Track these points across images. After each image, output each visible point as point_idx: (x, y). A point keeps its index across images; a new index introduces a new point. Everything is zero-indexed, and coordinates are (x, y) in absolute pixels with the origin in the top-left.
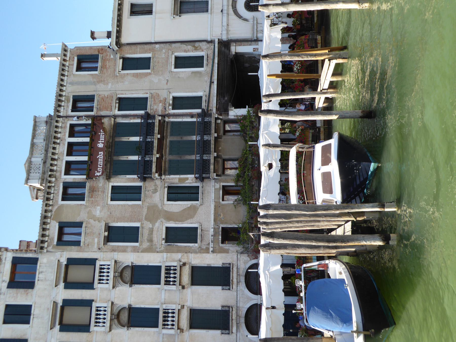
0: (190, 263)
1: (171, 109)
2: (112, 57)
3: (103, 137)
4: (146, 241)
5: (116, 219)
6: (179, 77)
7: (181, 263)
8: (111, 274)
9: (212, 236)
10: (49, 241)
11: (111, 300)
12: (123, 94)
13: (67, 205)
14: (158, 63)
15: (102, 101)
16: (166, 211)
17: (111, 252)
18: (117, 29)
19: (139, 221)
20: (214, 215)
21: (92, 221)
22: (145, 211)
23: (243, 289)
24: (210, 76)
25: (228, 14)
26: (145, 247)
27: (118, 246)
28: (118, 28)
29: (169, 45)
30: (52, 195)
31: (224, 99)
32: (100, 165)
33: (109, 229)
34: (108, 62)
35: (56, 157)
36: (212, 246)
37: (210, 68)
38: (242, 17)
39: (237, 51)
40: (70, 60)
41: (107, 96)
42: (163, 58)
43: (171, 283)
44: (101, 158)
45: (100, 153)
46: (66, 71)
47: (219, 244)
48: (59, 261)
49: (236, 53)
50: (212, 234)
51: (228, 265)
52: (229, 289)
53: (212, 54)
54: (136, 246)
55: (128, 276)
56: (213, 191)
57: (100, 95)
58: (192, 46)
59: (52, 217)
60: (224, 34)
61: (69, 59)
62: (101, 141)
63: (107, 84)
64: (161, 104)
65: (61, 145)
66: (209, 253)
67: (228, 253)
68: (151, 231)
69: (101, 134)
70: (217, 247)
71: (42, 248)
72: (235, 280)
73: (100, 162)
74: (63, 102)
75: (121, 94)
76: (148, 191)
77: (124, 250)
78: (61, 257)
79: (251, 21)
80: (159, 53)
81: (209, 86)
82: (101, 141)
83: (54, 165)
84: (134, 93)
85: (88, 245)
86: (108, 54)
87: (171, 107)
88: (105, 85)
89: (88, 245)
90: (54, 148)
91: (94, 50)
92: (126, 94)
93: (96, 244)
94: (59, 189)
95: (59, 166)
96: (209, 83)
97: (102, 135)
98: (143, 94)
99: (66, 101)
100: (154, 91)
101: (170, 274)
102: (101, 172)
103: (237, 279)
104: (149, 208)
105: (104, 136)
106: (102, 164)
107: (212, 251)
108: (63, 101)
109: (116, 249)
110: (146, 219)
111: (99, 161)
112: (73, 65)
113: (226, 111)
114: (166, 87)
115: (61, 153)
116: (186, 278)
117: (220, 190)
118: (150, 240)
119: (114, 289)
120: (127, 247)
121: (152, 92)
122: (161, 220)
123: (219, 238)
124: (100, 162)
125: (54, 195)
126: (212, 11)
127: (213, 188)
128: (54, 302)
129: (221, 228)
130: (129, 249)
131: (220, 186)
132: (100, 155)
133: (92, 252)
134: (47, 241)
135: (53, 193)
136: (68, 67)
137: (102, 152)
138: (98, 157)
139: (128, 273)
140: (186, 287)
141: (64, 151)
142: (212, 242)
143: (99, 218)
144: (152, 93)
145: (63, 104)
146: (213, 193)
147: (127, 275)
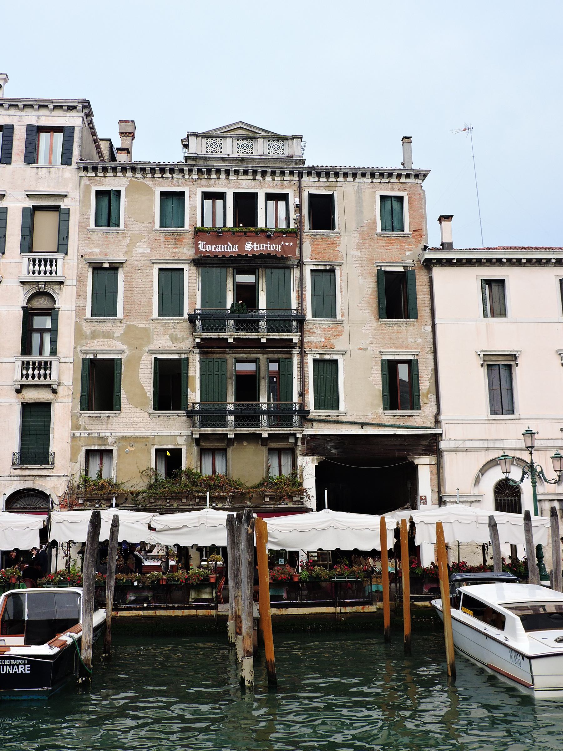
0: (56, 400)
1: (314, 358)
2: (408, 253)
3: (263, 247)
4: (94, 328)
5: (129, 278)
6: (372, 368)
7: (55, 387)
8: (42, 278)
9: (99, 434)
10: (97, 178)
11: (3, 280)
12: (341, 276)
13: (153, 201)
14: (398, 332)
15: (328, 243)
16: (140, 358)
17: (78, 275)
18: (454, 259)
19: (125, 315)
20: (132, 437)
21: (127, 241)
22: (141, 324)
23: (13, 486)
24: (374, 422)
25: (487, 450)
26: (83, 327)
27: (86, 285)
28: (455, 261)
29: (430, 349)
30: (170, 176)
31: (333, 447)
32: (215, 248)
33: (114, 268)
34: (398, 247)
35: (232, 177)
36: (82, 435)
37: (389, 421)
38: (482, 475)
39: (419, 467)
40: (400, 185)
41: (338, 251)
42: (407, 340)
43: (25, 372)
44: (227, 249)
45: (237, 246)
46: (381, 179)
47: (85, 445)
48: (66, 196)
49: (417, 465)
50: (101, 434)
51: (51, 460)
52: (13, 464)
53: (415, 425)
54: (85, 314)
55: (40, 304)
56: (172, 434)
57: (338, 238)
58: (429, 388)
59: (135, 180)
60: (449, 443)
61: (402, 183)
62: (257, 247)
63: (359, 249)
64: (323, 340)
65: (253, 183)
66: (71, 430)
67: (71, 460)
68: (109, 336)
69: (269, 245)
70: (81, 443)
71: (86, 169)
72: (27, 473)
73: (221, 247)
74: (326, 180)
75: (341, 273)
76: (174, 328)
77: (80, 295)
78: (72, 198)
79: (476, 491)
80: (417, 333)
81: (356, 421)
82: (257, 247)
83: (218, 175)
84: (343, 294)
85: (89, 238)
86: (413, 247)
87: (318, 357)
88: (357, 245)
89: (89, 238)
90: (246, 173)
91: (419, 223)
92: (341, 280)
93: (90, 251)
94: (178, 186)
95: (217, 181)
96: (361, 421)
97: (266, 247)
98: (341, 309)
99: (328, 184)
100: (346, 328)
101: (39, 370)
102: (204, 250)
103: (29, 476)
104: (146, 329)
105: (265, 249)
106: (217, 250)
107: (74, 434)
108: (328, 180)
109: (82, 283)
110: (128, 326)
111: (223, 246)
112: (392, 190)
113: (310, 452)
114: (354, 347)
115: (239, 184)
116: (32, 396)
117: (174, 445)
118: (94, 336)
119: (20, 284)
120: (85, 299)
121: (345, 324)
122: (126, 351)
123: (95, 445)
124: (221, 247)
125: (170, 179)
126: (494, 422)
127: (176, 434)
128: (4, 195)
129: (111, 448)
130: (81, 303)
131: (181, 445)
132: (233, 247)
133: (78, 244)
134: (96, 175)
135: (172, 178)
136: (388, 183)
137: (237, 250)
138: (229, 243)
139: (45, 303)
140: (20, 395)
141: (242, 188)
142: (89, 434)
143: (132, 252)
144: (343, 325)
145: (323, 179)
146: (169, 434)
147: (41, 302)
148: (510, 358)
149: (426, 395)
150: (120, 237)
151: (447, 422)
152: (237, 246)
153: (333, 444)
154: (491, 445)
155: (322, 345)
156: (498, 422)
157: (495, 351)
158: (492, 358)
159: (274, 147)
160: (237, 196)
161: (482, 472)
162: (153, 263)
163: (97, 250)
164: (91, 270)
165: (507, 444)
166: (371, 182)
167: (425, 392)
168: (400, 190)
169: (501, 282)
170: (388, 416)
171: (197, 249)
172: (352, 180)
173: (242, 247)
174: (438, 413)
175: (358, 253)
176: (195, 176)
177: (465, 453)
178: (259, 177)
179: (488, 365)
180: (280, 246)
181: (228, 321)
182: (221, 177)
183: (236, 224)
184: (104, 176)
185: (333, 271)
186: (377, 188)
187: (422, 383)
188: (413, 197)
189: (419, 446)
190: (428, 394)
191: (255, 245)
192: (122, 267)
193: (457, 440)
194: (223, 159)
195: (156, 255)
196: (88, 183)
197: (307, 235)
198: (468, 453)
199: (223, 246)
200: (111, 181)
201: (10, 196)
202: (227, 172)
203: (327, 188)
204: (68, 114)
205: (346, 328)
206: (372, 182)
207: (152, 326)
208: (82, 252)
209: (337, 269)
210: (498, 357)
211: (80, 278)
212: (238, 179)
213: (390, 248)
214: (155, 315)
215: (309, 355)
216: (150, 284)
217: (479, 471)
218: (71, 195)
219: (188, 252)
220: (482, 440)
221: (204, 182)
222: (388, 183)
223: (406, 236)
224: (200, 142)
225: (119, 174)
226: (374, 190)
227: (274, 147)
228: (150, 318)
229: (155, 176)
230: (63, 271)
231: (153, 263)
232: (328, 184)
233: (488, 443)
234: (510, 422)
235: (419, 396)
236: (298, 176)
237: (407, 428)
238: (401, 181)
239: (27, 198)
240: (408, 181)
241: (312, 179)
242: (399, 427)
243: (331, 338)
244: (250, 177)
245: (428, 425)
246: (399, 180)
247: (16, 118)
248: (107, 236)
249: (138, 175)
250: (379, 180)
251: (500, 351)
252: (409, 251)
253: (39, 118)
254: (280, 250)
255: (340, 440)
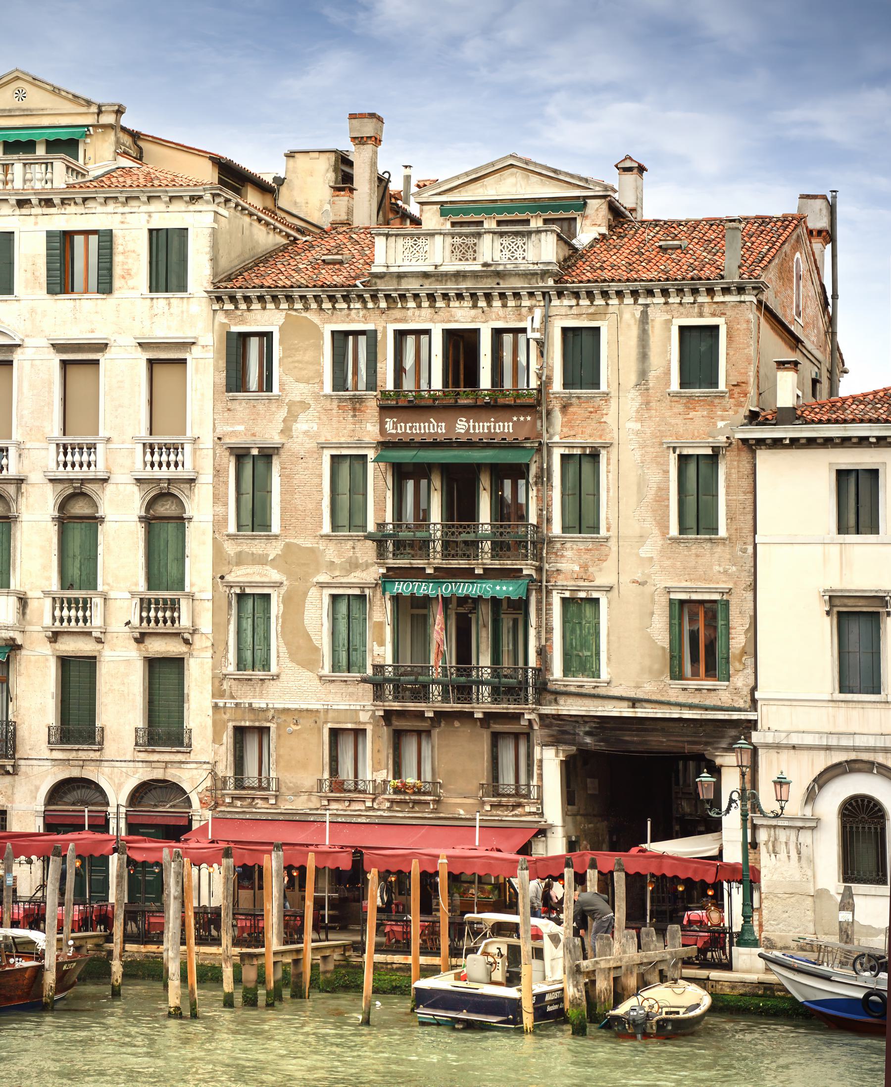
0: (191, 655)
1: (563, 596)
2: (720, 424)
3: (483, 429)
4: (239, 549)
5: (287, 472)
6: (652, 614)
7: (187, 636)
8: (164, 473)
9: (250, 704)
10: (239, 313)
11: (112, 476)
12: (608, 464)
13: (319, 348)
14: (697, 556)
15: (590, 409)
16: (305, 594)
17: (214, 468)
19: (284, 527)
20: (296, 710)
21: (283, 413)
22: (307, 542)
23: (137, 776)
24: (654, 698)
25: (828, 748)
26: (225, 546)
27: (226, 483)
29: (749, 583)
30: (345, 306)
31: (588, 733)
32: (411, 428)
33: (267, 455)
34: (705, 413)
35: (440, 304)
36: (228, 705)
37: (677, 697)
38: (820, 788)
39: (723, 770)
40: (715, 306)
41: (605, 422)
42: (712, 569)
43: (144, 614)
44: (429, 429)
45: (443, 424)
46: (682, 298)
47: (233, 721)
48: (194, 343)
49: (722, 766)
50: (254, 705)
51: (186, 741)
52: (136, 745)
53: (719, 703)
54: (227, 526)
55: (166, 509)
56: (352, 707)
57: (606, 401)
58: (744, 647)
59: (294, 313)
60: (765, 737)
61: (717, 303)
62: (474, 427)
63: (640, 420)
64: (577, 568)
65: (473, 312)
66: (213, 696)
67: (214, 741)
68: (261, 560)
69: (492, 424)
70: (226, 717)
71: (219, 299)
72: (155, 757)
73: (420, 427)
74: (588, 303)
75: (608, 459)
76: (354, 548)
77: (218, 498)
78: (203, 347)
79: (808, 812)
80: (728, 556)
81: (624, 695)
82: (474, 427)
83: (418, 300)
84: (611, 494)
85: (229, 410)
86: (731, 413)
87: (567, 594)
88: (637, 412)
89: (229, 410)
90: (460, 297)
91: (743, 371)
92: (608, 472)
93: (231, 429)
94: (359, 322)
95: (417, 312)
96: (632, 694)
97: (489, 428)
98: (607, 518)
99: (592, 310)
100: (614, 549)
101: (165, 611)
102: (394, 431)
103: (158, 762)
104: (312, 550)
105: (486, 431)
106: (414, 432)
107: (216, 704)
108: (592, 302)
109: (221, 479)
110: (288, 545)
111: (422, 425)
112: (701, 315)
113: (555, 742)
114: (625, 579)
115: (451, 316)
116: (159, 647)
117: (355, 723)
118: (240, 560)
119: (134, 482)
120: (226, 504)
121: (613, 543)
122: (285, 583)
123: (245, 721)
124: (420, 427)
125: (346, 311)
126: (843, 705)
127: (358, 708)
128: (107, 344)
129: (268, 725)
130: (220, 509)
131: (365, 723)
132: (438, 426)
133: (214, 420)
134: (237, 308)
135: (349, 308)
136: (694, 303)
137: (444, 431)
138: (432, 420)
139: (173, 508)
140: (142, 646)
141: (456, 321)
142: (237, 704)
143: (291, 430)
144: (609, 544)
145: (585, 302)
146: (347, 707)
147: (168, 507)
148: (878, 602)
149: (739, 657)
150: (274, 407)
151: (766, 703)
152: (443, 424)
153: (587, 729)
154: (833, 741)
155: (575, 576)
156: (850, 705)
157: (849, 591)
158: (846, 601)
159: (510, 247)
160: (450, 335)
161: (820, 782)
162: (323, 448)
163: (241, 428)
164: (233, 460)
165: (860, 742)
166: (665, 304)
167: (737, 652)
168: (714, 315)
169: (874, 474)
170: (674, 691)
171: (383, 430)
172: (631, 301)
173: (451, 427)
174: (754, 688)
175: (638, 426)
176: (383, 304)
177: (792, 751)
178: (482, 303)
179: (839, 613)
180: (511, 424)
181: (399, 584)
182: (423, 305)
183: (445, 384)
184: (249, 310)
185: (594, 456)
186: (675, 314)
187: (733, 638)
188: (736, 327)
189: (723, 737)
190: (742, 656)
191: (471, 424)
192: (277, 454)
193: (779, 731)
194: (426, 275)
195: (328, 435)
196: (226, 321)
197: (556, 398)
198: (797, 752)
199: (422, 425)
200: (259, 317)
201: (115, 344)
202: (431, 297)
203: (591, 317)
204: (192, 208)
205: (614, 549)
206: (666, 303)
207: (322, 545)
208: (219, 432)
209: (603, 454)
210: (857, 600)
211: (218, 472)
212: (449, 306)
213: (690, 416)
214: (327, 528)
215: (554, 592)
216: (317, 480)
217: (814, 781)
218: (201, 342)
219: (370, 431)
220: (818, 733)
221: (397, 314)
222: (694, 303)
223: (721, 396)
224: (393, 245)
225: (270, 306)
226: (669, 317)
227: (510, 247)
228: (318, 533)
229: (324, 306)
230: (194, 461)
231: (323, 448)
232: (592, 310)
233: (827, 738)
234: (870, 705)
235: (728, 658)
236: (544, 298)
237: (706, 708)
238: (717, 299)
239: (139, 349)
240: (728, 298)
241: (566, 302)
242: (691, 707)
243: (590, 563)
244: (468, 303)
245: (741, 704)
246: (712, 298)
247: (118, 217)
248: (254, 406)
249: (298, 305)
250: (678, 300)
251: (856, 591)
252: (723, 420)
253: (150, 216)
254: (511, 431)
255: (598, 723)
